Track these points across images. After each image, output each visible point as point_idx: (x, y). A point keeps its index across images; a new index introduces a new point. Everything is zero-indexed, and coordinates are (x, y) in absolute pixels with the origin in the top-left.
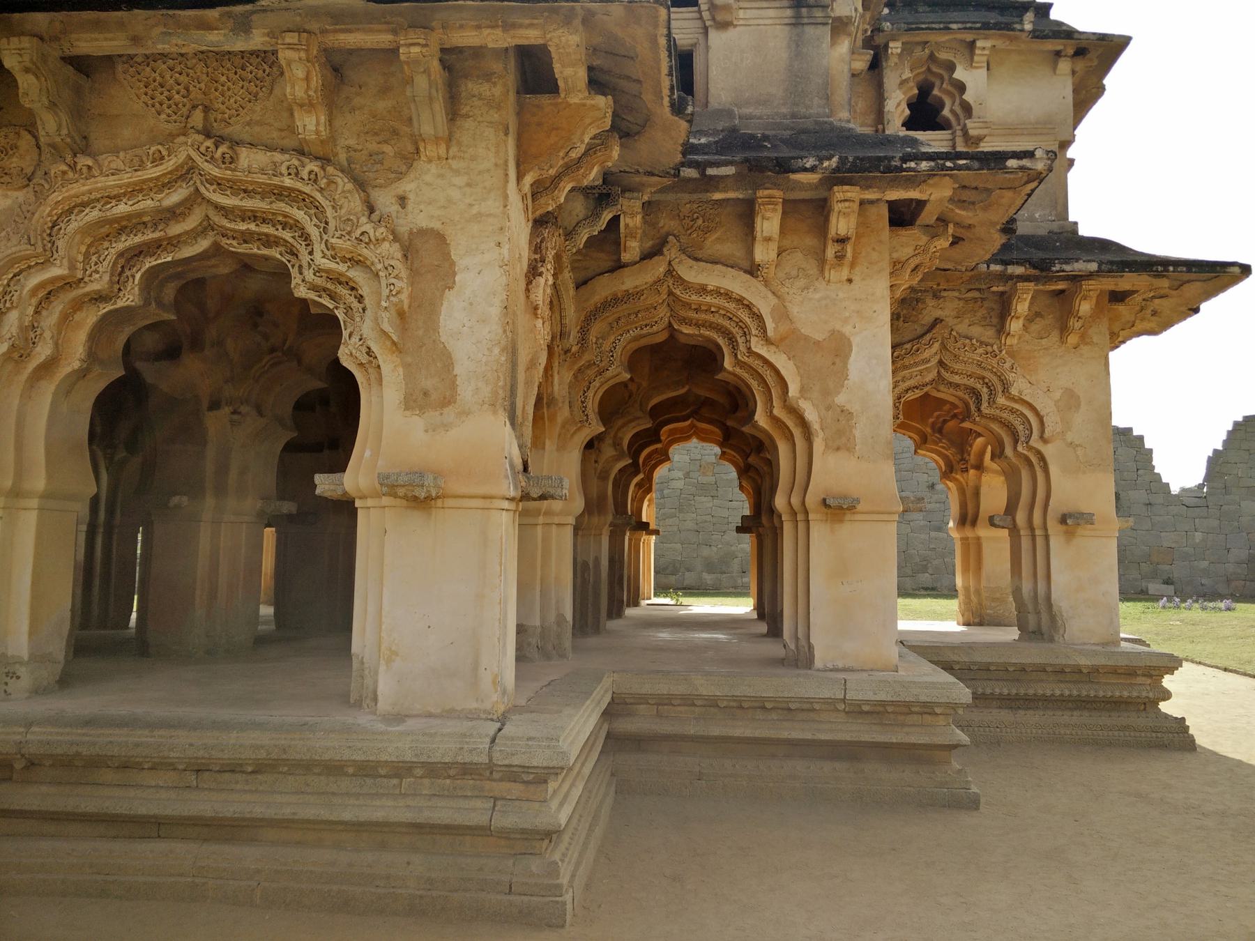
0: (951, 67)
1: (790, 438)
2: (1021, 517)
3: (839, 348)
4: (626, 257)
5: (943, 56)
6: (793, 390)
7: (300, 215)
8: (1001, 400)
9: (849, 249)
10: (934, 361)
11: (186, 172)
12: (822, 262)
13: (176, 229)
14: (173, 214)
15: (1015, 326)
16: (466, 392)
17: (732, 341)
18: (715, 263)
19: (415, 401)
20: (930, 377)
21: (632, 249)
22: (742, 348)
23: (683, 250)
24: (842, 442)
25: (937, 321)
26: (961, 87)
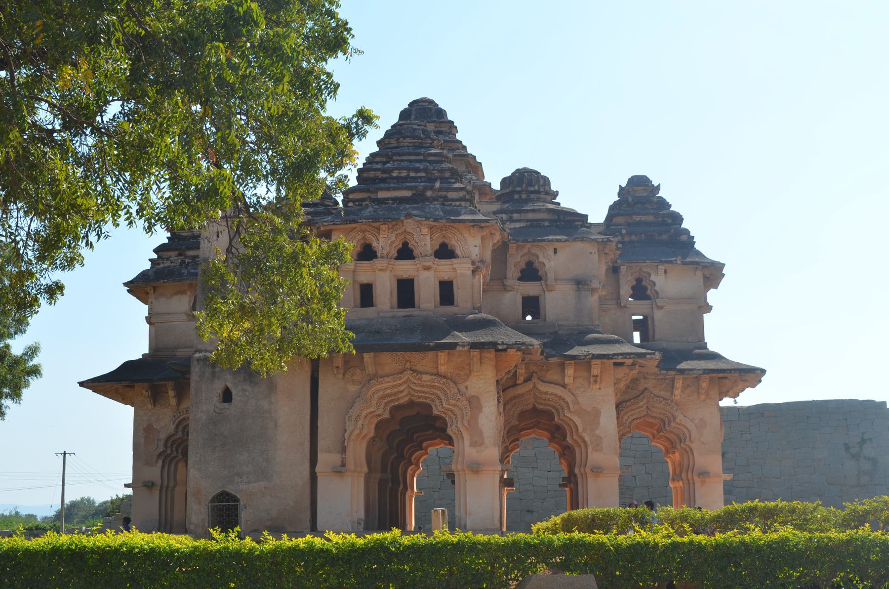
0: (650, 275)
1: (580, 447)
3: (597, 414)
4: (518, 382)
5: (645, 270)
6: (580, 429)
7: (438, 392)
8: (673, 424)
9: (598, 379)
10: (645, 407)
11: (405, 382)
12: (589, 383)
13: (401, 395)
14: (401, 392)
15: (677, 392)
16: (488, 441)
17: (557, 411)
18: (550, 383)
19: (474, 444)
20: (645, 413)
21: (521, 379)
22: (561, 414)
23: (539, 379)
25: (646, 389)
26: (654, 284)
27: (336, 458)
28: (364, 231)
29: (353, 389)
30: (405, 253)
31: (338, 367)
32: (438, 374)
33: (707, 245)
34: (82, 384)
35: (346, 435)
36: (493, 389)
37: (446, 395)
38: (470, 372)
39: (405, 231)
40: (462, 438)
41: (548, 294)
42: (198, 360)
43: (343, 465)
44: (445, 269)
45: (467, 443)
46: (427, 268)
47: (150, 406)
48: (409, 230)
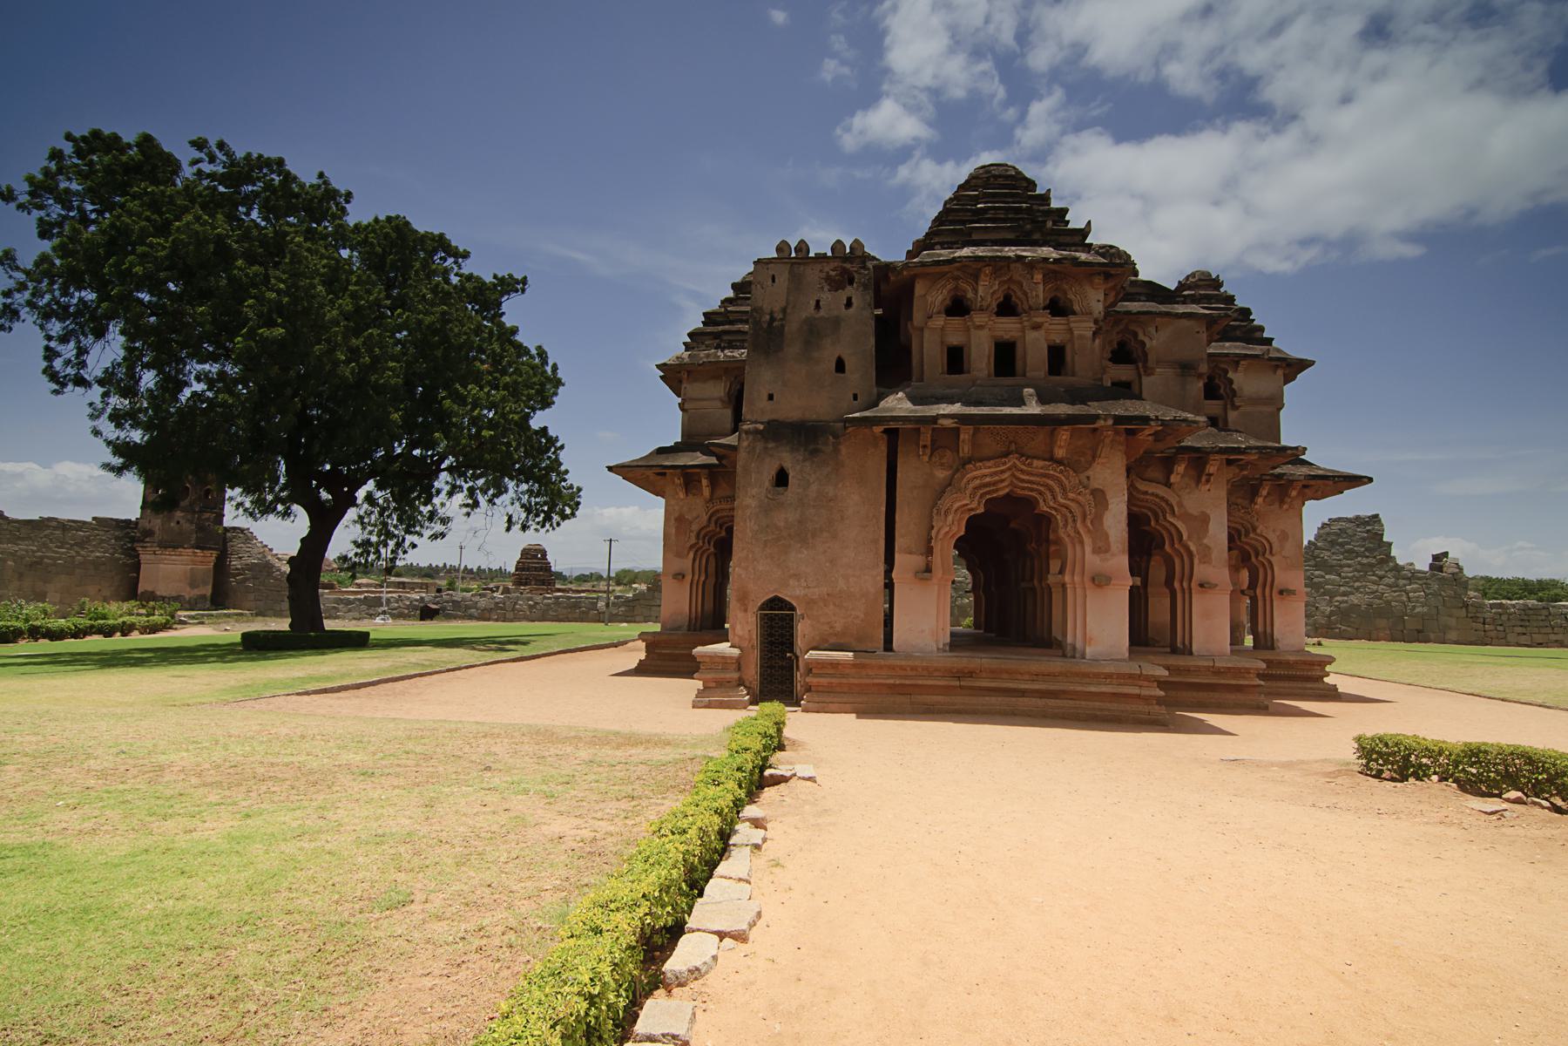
2: (1259, 591)
3: (1204, 520)
15: (1260, 500)
24: (1206, 557)
26: (1231, 382)
27: (918, 561)
28: (956, 279)
29: (941, 474)
30: (1007, 308)
31: (925, 447)
32: (1052, 459)
33: (1287, 344)
34: (610, 469)
35: (933, 533)
36: (1122, 481)
37: (1064, 489)
38: (1094, 458)
39: (1010, 279)
40: (1082, 543)
41: (1145, 380)
42: (747, 432)
43: (928, 570)
44: (1055, 329)
45: (1088, 549)
46: (1037, 327)
47: (682, 495)
48: (1017, 277)
